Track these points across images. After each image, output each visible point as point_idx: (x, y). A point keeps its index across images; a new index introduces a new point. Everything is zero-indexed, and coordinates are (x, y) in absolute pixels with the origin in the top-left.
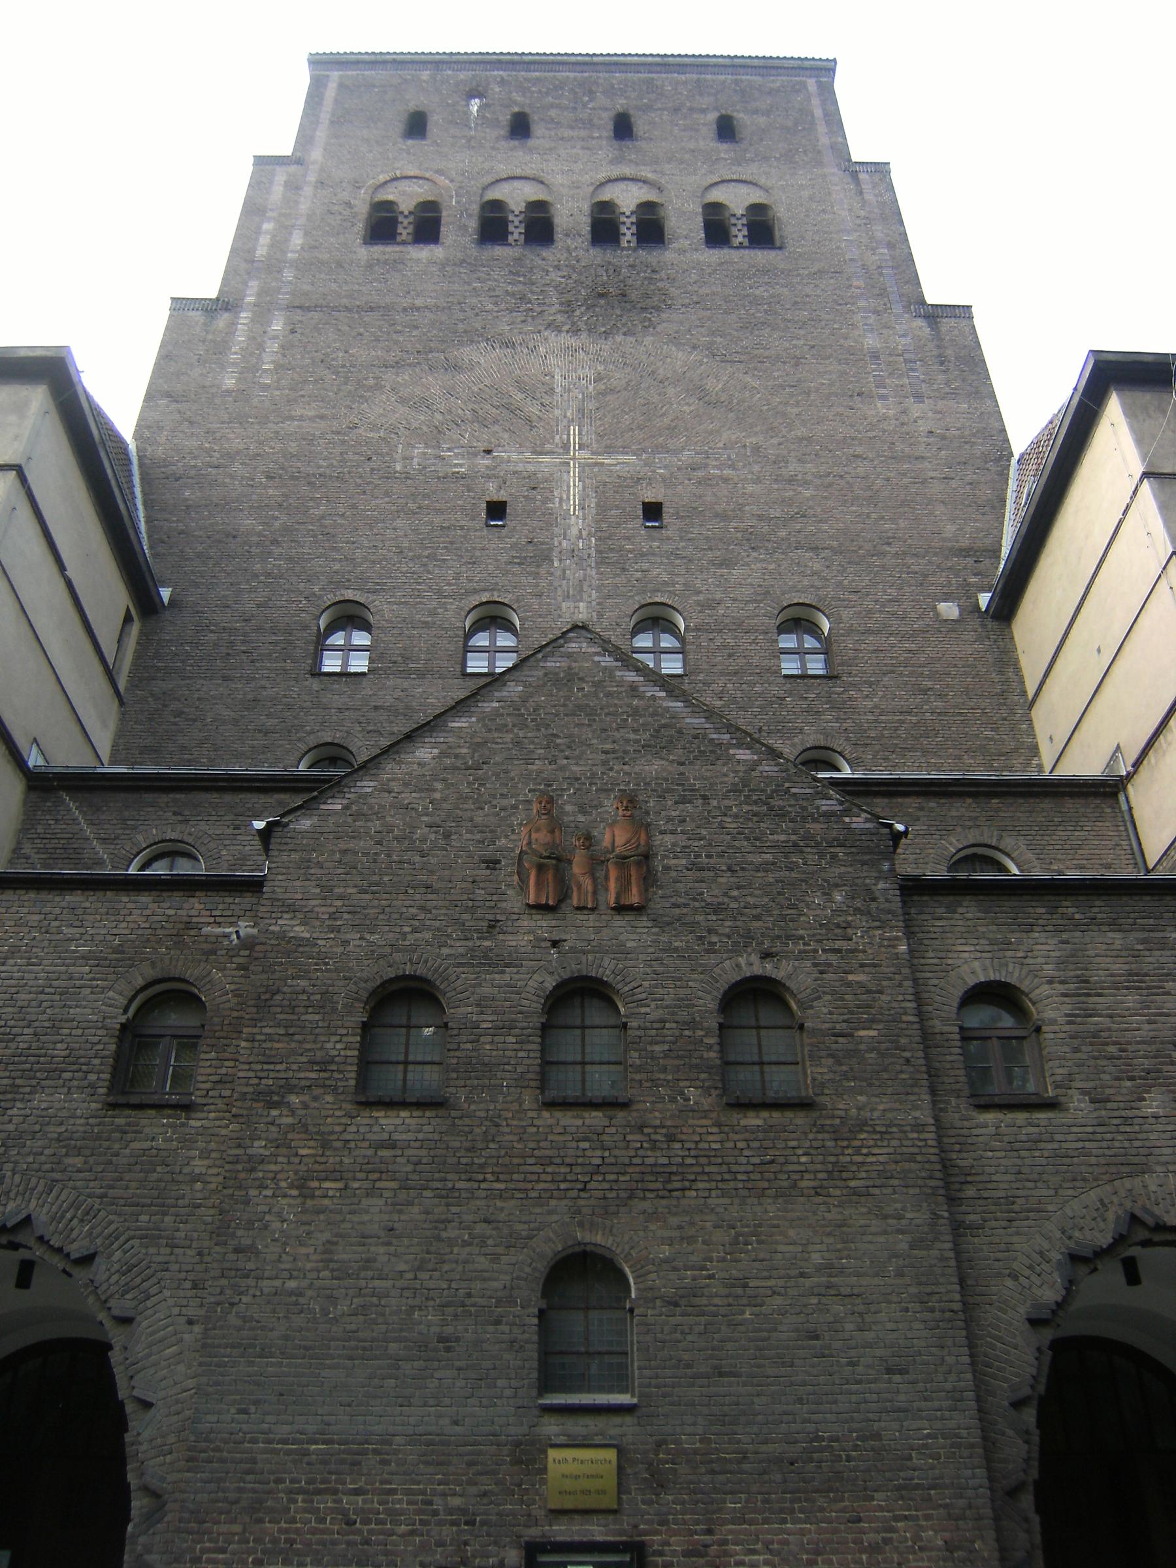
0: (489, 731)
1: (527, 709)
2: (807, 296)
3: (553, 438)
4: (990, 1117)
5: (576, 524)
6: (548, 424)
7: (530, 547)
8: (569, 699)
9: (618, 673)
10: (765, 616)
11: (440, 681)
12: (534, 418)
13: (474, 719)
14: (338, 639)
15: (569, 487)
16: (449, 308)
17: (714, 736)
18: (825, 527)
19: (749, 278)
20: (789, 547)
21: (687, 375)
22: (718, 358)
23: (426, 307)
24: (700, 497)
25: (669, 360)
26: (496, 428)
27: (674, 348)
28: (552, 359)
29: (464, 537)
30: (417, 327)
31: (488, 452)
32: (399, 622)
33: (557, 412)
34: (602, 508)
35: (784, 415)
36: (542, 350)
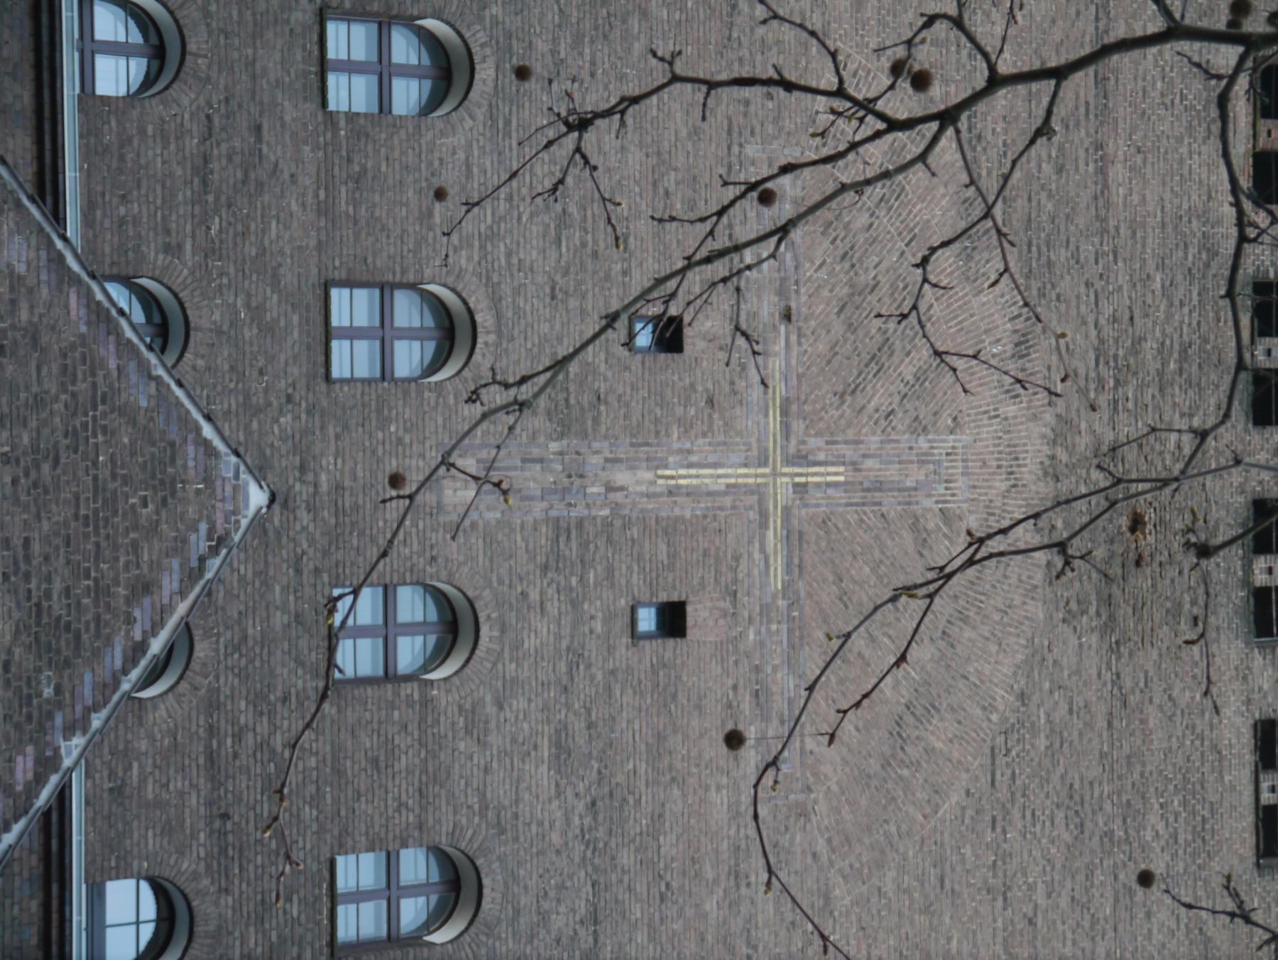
0: (65, 356)
1: (104, 415)
2: (1149, 915)
3: (819, 434)
5: (634, 480)
6: (849, 425)
7: (586, 399)
8: (125, 483)
9: (175, 563)
10: (457, 824)
11: (313, 243)
12: (860, 399)
13: (83, 329)
14: (404, 49)
15: (715, 465)
16: (1105, 231)
17: (59, 720)
18: (641, 937)
19: (1184, 803)
20: (596, 869)
21: (961, 684)
22: (1000, 740)
23: (1106, 186)
24: (699, 707)
25: (993, 648)
26: (838, 328)
27: (1020, 657)
28: (989, 430)
29: (608, 277)
30: (1060, 170)
31: (787, 316)
32: (430, 164)
33: (874, 441)
34: (669, 529)
35: (880, 865)
36: (1011, 409)
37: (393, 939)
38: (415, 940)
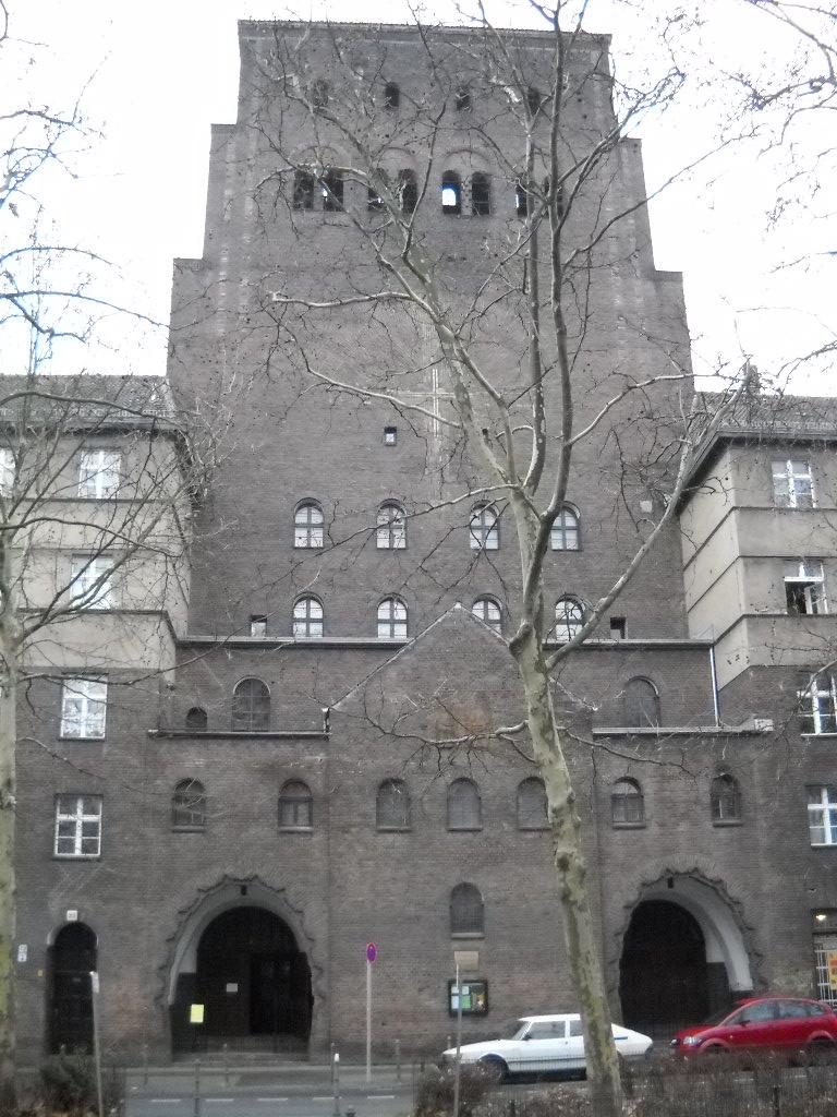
4: (618, 833)
37: (578, 529)
38: (578, 521)
